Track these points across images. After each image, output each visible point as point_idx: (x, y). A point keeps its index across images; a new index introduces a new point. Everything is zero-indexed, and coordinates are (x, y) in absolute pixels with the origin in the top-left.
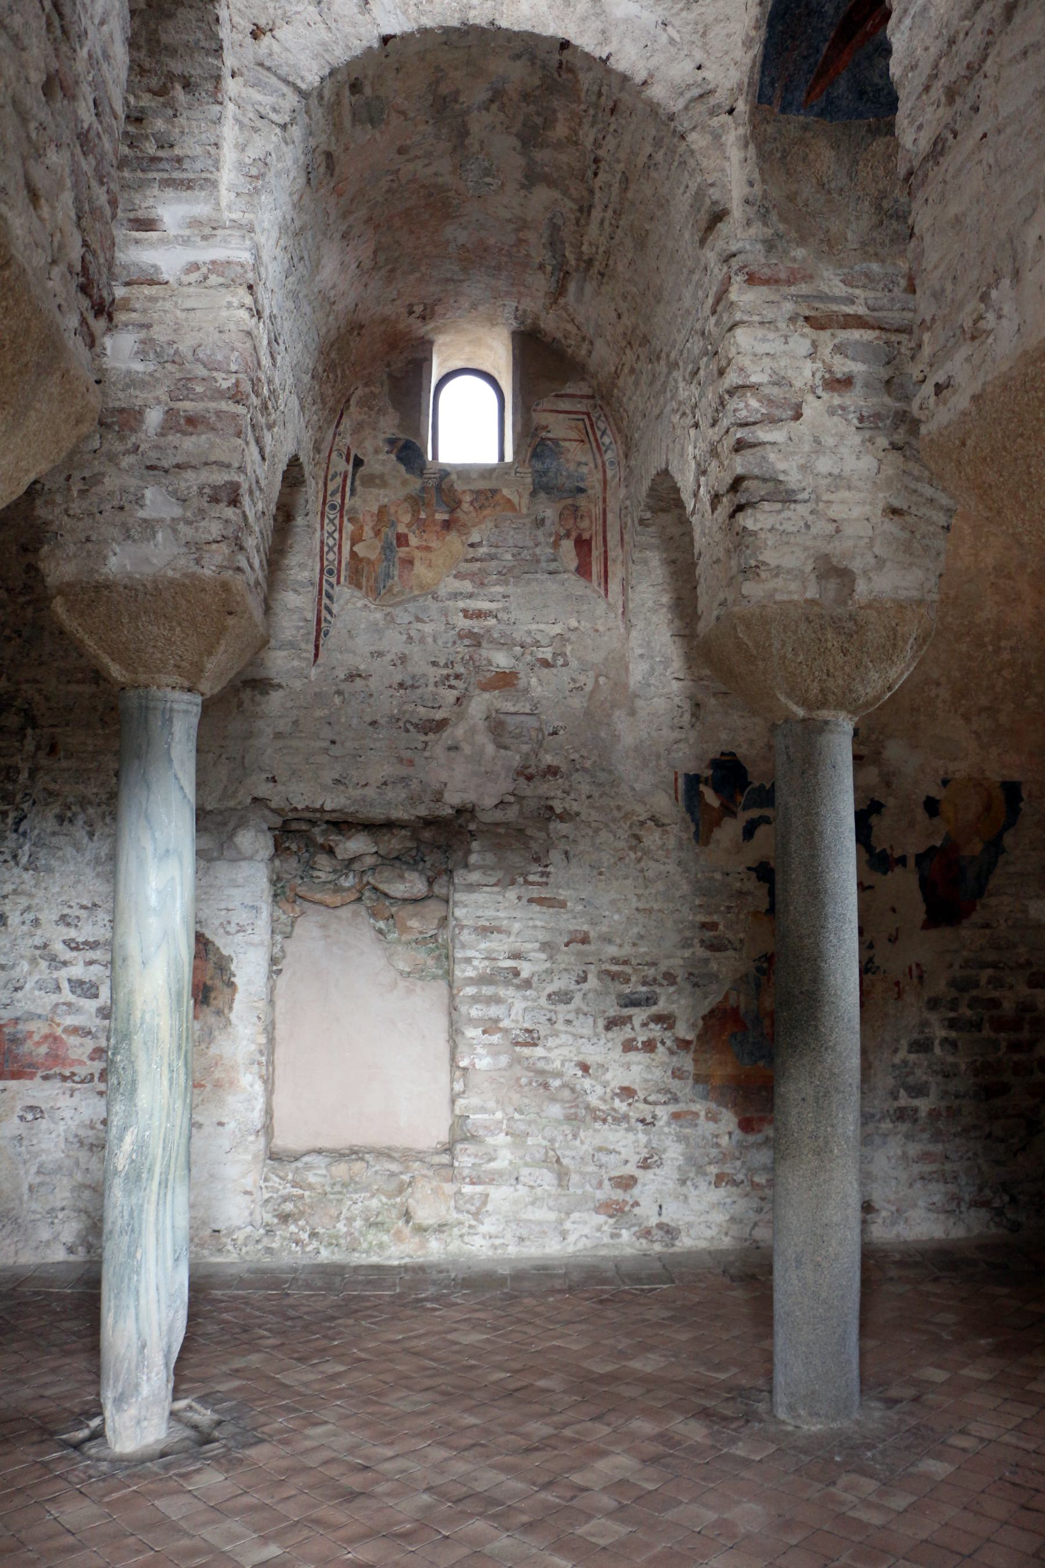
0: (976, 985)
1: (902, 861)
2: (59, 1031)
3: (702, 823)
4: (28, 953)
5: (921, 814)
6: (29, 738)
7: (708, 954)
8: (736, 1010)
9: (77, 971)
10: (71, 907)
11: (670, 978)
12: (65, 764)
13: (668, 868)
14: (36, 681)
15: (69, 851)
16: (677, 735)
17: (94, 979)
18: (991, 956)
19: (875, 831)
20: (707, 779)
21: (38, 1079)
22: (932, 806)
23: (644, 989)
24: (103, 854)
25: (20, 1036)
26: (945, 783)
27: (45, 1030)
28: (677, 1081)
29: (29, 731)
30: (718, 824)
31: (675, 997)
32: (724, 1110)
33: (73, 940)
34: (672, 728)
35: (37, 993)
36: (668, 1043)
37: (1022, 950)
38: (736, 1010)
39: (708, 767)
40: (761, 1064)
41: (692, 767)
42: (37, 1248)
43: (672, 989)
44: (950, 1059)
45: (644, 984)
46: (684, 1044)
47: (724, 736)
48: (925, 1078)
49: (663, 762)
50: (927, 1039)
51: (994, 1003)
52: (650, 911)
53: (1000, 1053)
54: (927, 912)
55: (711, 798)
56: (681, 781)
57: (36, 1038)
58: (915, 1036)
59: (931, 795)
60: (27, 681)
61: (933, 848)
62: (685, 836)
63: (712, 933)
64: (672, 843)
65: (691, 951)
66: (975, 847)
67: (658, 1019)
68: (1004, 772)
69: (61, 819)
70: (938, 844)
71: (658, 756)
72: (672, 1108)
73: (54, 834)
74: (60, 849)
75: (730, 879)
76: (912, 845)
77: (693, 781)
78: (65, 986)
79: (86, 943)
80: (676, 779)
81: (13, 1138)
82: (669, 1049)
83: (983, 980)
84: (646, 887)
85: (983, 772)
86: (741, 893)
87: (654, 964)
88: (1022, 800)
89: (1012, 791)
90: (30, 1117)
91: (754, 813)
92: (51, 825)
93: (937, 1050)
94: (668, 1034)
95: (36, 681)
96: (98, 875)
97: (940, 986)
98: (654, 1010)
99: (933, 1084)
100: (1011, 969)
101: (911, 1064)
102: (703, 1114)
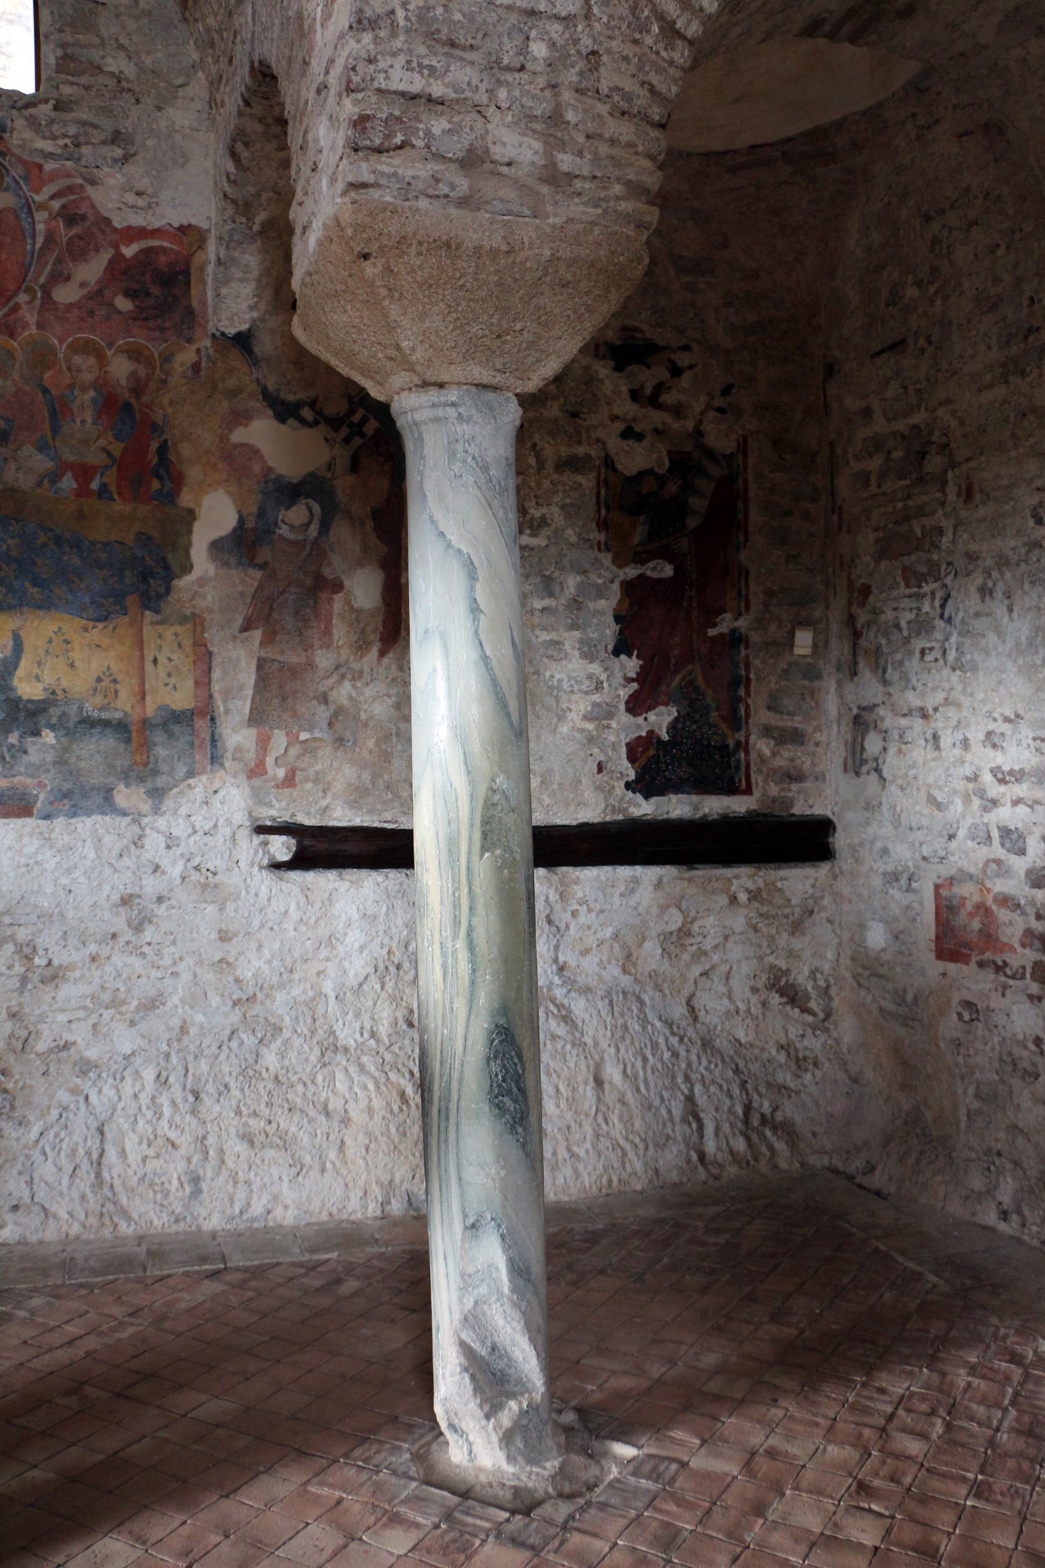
2: (990, 902)
4: (961, 785)
6: (951, 483)
9: (1004, 814)
10: (995, 720)
12: (983, 511)
14: (948, 401)
15: (992, 638)
17: (1020, 826)
21: (973, 964)
24: (1023, 639)
25: (955, 902)
27: (977, 898)
29: (950, 475)
33: (999, 768)
35: (970, 843)
42: (967, 1198)
57: (969, 907)
60: (941, 404)
69: (985, 592)
73: (977, 615)
74: (983, 636)
78: (995, 834)
79: (1011, 772)
81: (951, 1041)
90: (967, 1016)
92: (973, 603)
95: (948, 401)
96: (1020, 671)
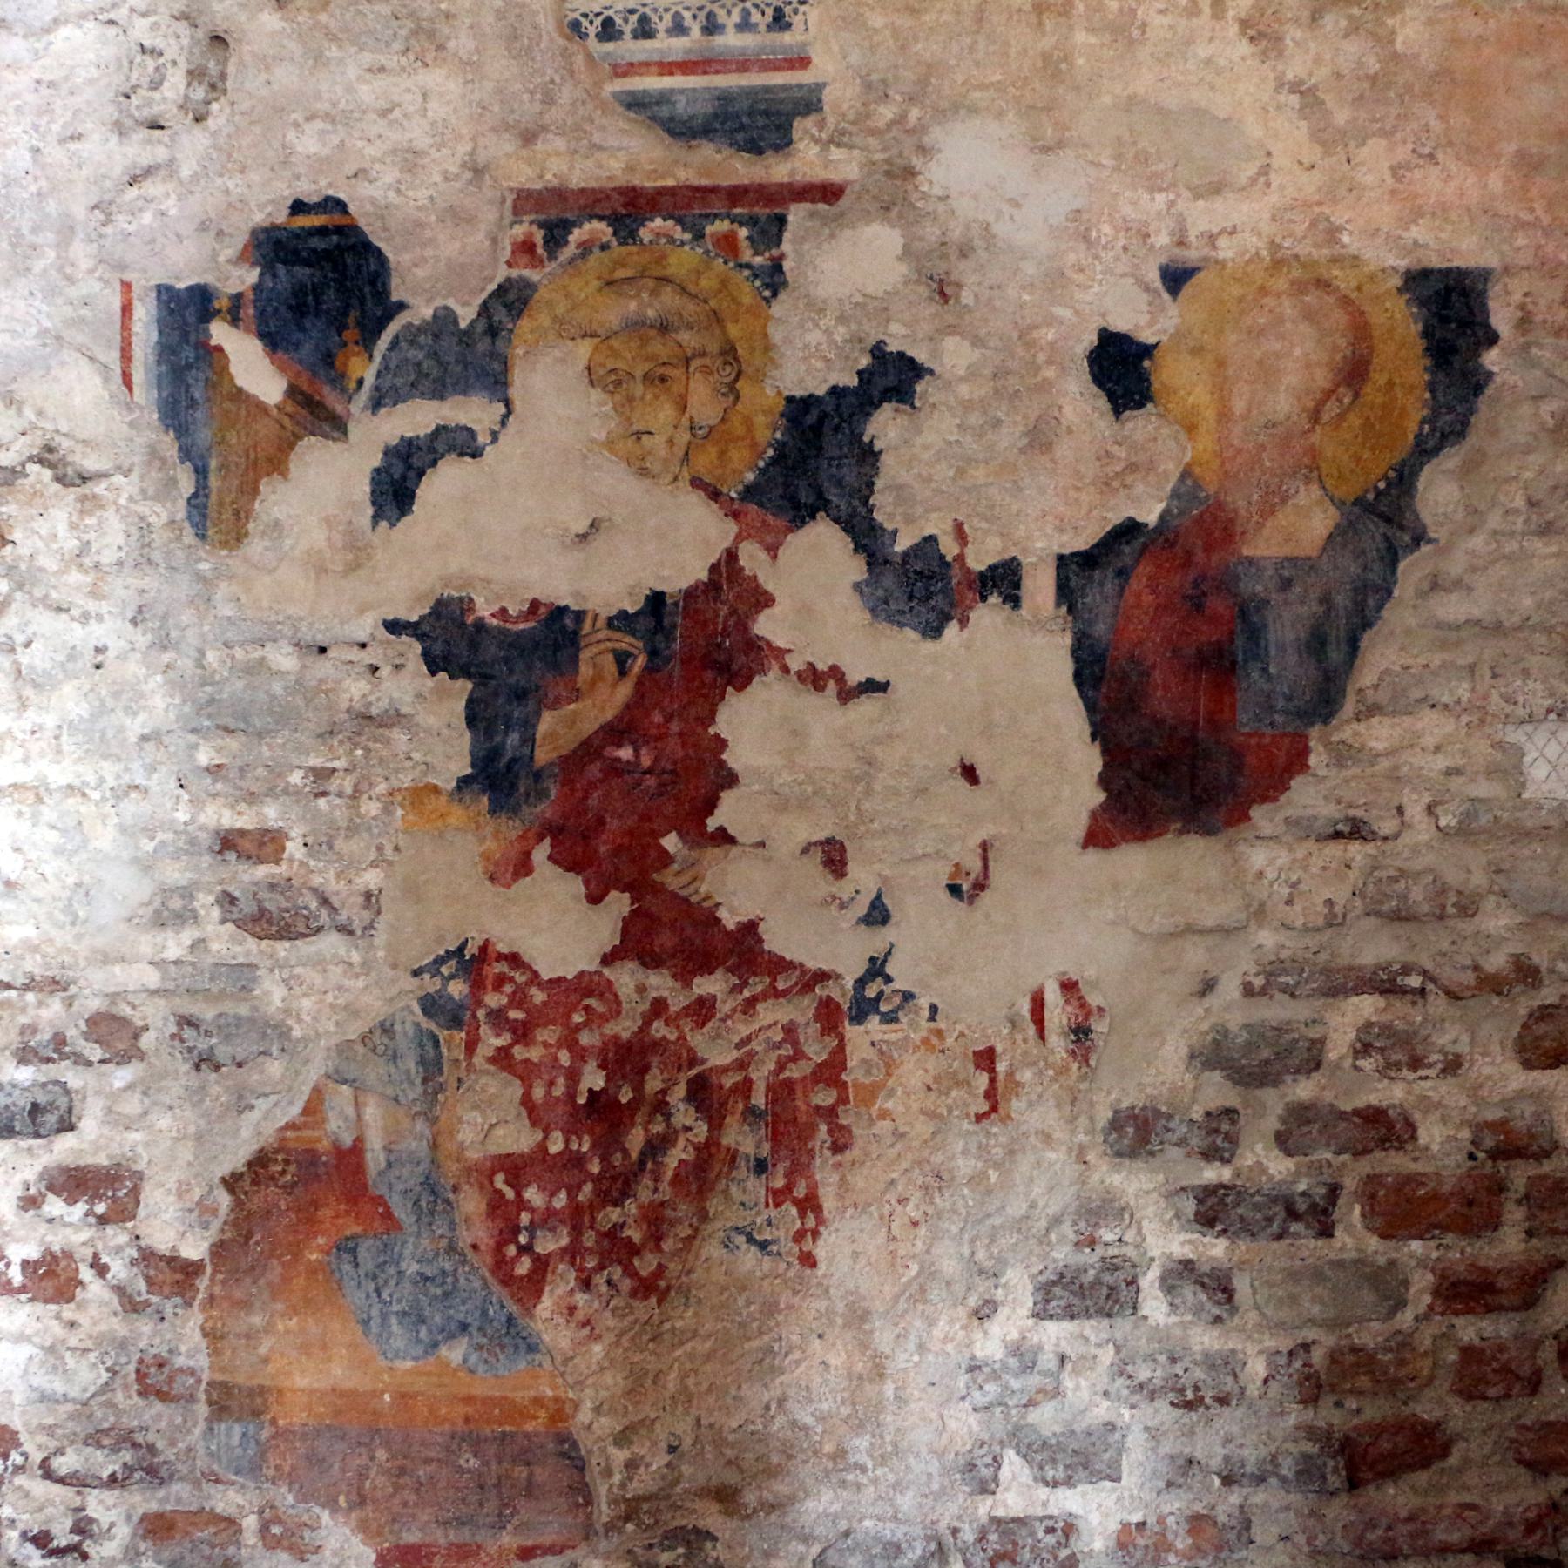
0: (1313, 1063)
1: (1003, 581)
3: (218, 469)
5: (1078, 399)
7: (250, 948)
8: (350, 1158)
11: (114, 1033)
13: (99, 633)
16: (140, 150)
18: (1375, 948)
19: (891, 469)
20: (237, 299)
22: (1121, 368)
23: (25, 1074)
26: (1176, 278)
28: (158, 1406)
30: (276, 462)
31: (132, 1105)
32: (325, 1516)
34: (120, 129)
36: (119, 1269)
37: (1496, 920)
38: (350, 1158)
39: (242, 258)
40: (455, 1353)
41: (185, 264)
43: (122, 1076)
44: (1205, 1339)
45: (25, 1055)
46: (178, 1276)
47: (308, 143)
48: (1102, 1411)
49: (82, 254)
50: (1110, 1266)
51: (1384, 1128)
52: (37, 793)
53: (1406, 1318)
54: (1104, 781)
55: (254, 370)
56: (145, 314)
58: (1063, 1254)
59: (1120, 324)
61: (1129, 530)
62: (158, 514)
63: (262, 871)
64: (112, 538)
65: (188, 935)
66: (1304, 523)
67: (74, 1182)
68: (1416, 233)
70: (1150, 515)
71: (67, 231)
72: (144, 1501)
75: (323, 668)
76: (1044, 524)
77: (188, 310)
80: (127, 310)
82: (120, 1290)
83: (1340, 1044)
84: (24, 705)
85: (1333, 233)
86: (370, 722)
87: (56, 985)
88: (1492, 339)
89: (1451, 310)
91: (416, 418)
93: (1154, 1306)
94: (117, 1236)
97: (1159, 1063)
98: (64, 1149)
99: (1136, 1441)
100: (1453, 996)
101: (1048, 1361)
102: (250, 1523)
